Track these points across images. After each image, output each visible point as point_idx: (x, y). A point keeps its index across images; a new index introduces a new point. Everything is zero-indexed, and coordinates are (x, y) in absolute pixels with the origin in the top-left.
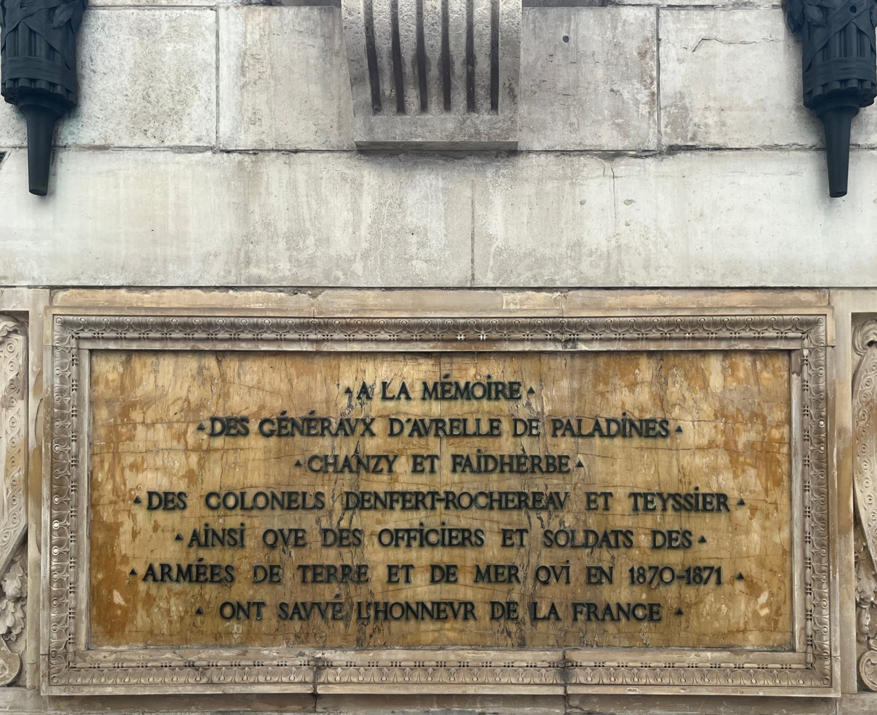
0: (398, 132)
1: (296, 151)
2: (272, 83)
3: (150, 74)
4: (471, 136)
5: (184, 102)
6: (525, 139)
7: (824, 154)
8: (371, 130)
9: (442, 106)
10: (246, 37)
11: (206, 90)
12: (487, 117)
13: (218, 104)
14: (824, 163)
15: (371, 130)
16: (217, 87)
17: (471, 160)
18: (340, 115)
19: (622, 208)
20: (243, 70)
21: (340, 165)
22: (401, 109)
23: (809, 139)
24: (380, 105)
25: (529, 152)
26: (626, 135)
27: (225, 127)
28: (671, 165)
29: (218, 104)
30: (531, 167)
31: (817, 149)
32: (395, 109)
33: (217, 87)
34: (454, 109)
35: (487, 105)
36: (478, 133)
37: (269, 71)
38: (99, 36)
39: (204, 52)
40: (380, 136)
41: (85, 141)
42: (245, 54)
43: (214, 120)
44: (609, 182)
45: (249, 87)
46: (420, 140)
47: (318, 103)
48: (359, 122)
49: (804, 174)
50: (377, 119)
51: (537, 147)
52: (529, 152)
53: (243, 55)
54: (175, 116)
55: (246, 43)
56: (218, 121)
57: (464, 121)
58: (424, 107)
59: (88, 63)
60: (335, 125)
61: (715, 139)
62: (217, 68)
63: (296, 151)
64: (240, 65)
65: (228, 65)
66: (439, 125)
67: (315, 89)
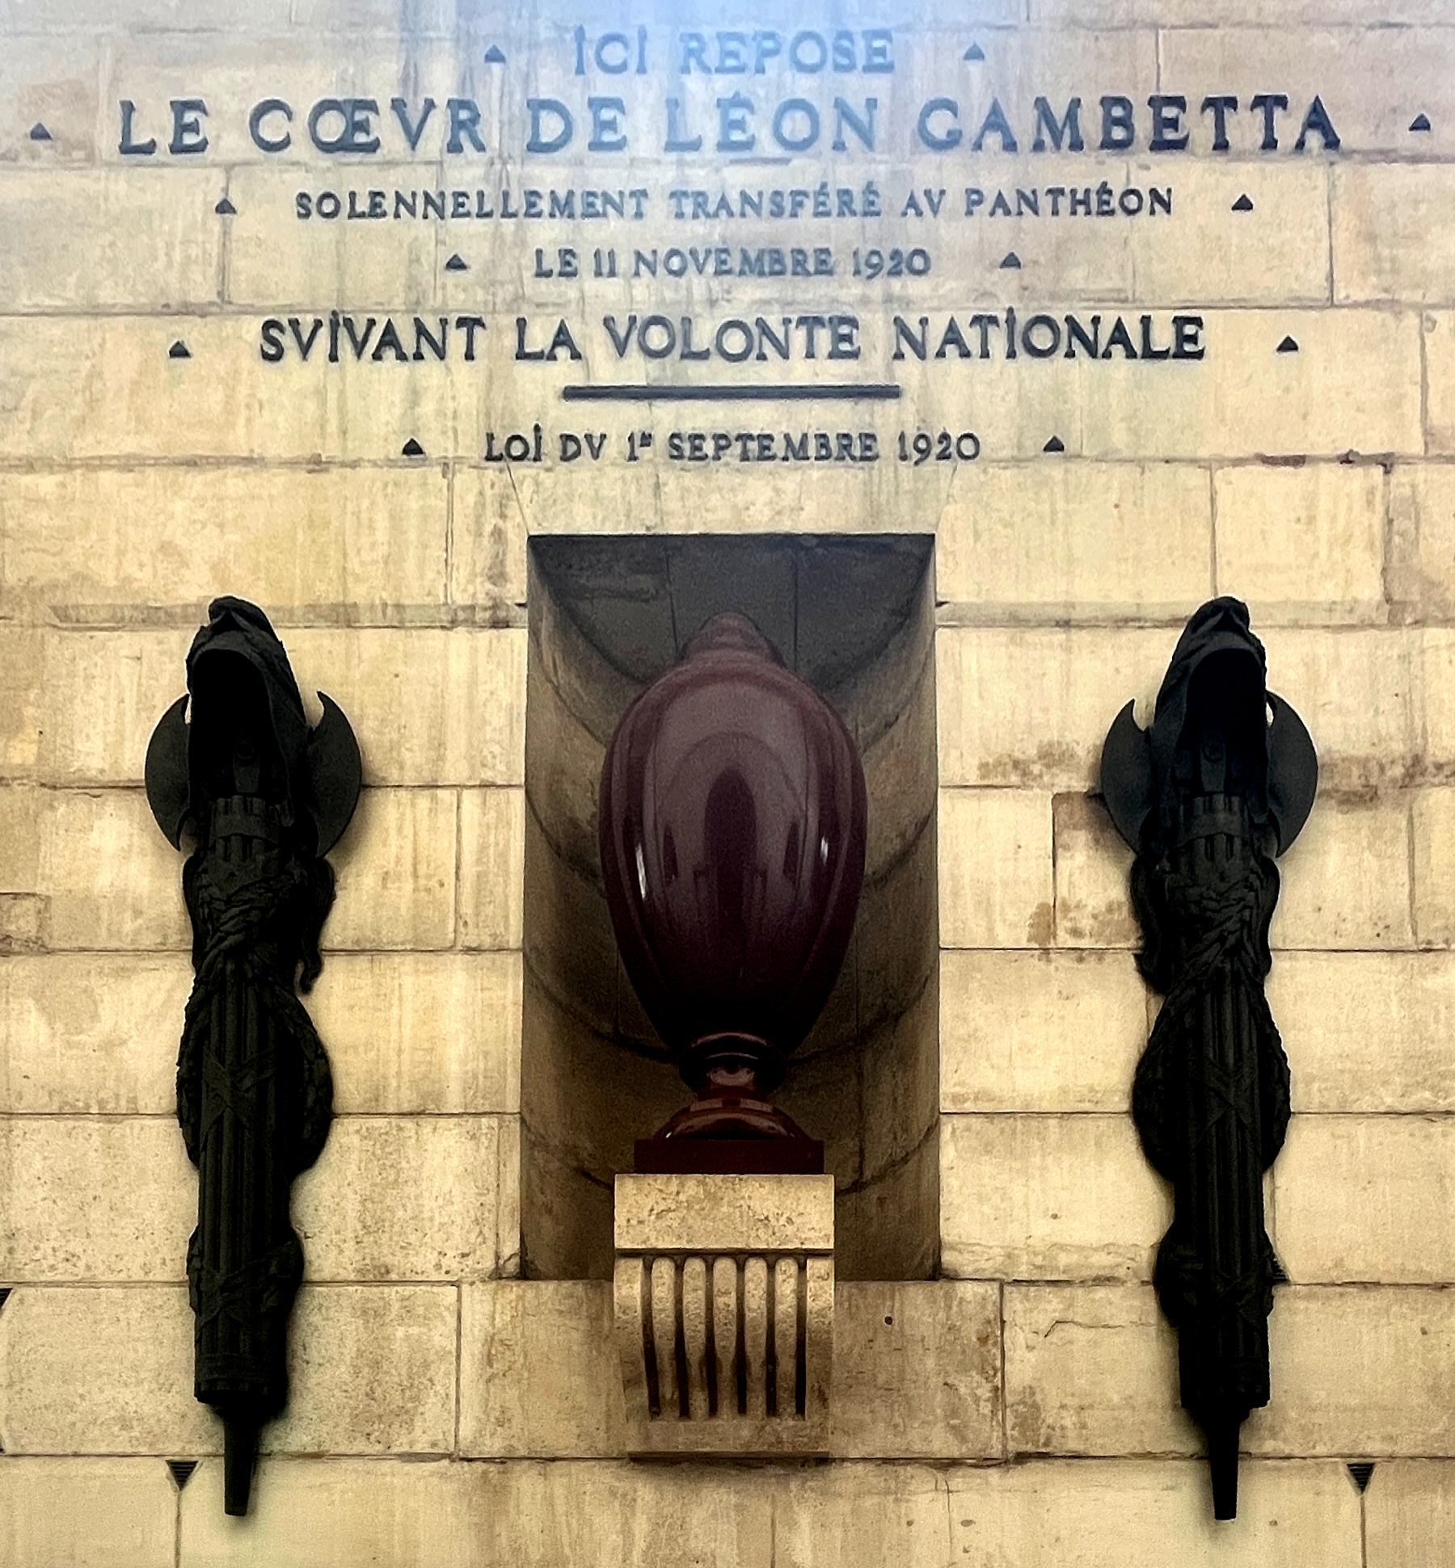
0: (680, 1439)
1: (554, 1460)
2: (526, 1375)
3: (376, 1365)
4: (771, 1445)
5: (416, 1399)
6: (836, 1444)
7: (1205, 1464)
8: (647, 1438)
9: (735, 1410)
10: (494, 1319)
11: (443, 1382)
12: (791, 1423)
13: (458, 1401)
14: (1208, 1474)
15: (647, 1438)
16: (458, 1380)
17: (771, 1470)
18: (609, 1416)
19: (960, 1530)
20: (489, 1360)
21: (605, 1477)
22: (685, 1412)
23: (1191, 1446)
24: (658, 1406)
25: (843, 1460)
26: (964, 1440)
27: (467, 1429)
28: (1020, 1477)
29: (458, 1401)
30: (846, 1478)
31: (1200, 1458)
32: (677, 1414)
33: (458, 1380)
34: (750, 1413)
35: (792, 1409)
36: (780, 1442)
37: (522, 1360)
38: (315, 1319)
39: (441, 1336)
40: (658, 1445)
41: (293, 1448)
42: (492, 1339)
43: (453, 1421)
44: (943, 1497)
45: (496, 1381)
46: (707, 1449)
47: (581, 1398)
48: (632, 1429)
49: (1176, 1494)
50: (656, 1427)
51: (854, 1454)
52: (843, 1460)
53: (490, 1340)
54: (405, 1416)
55: (494, 1327)
56: (457, 1422)
57: (763, 1427)
58: (713, 1411)
59: (300, 1352)
60: (603, 1427)
61: (1074, 1445)
62: (458, 1357)
63: (554, 1460)
64: (485, 1353)
65: (472, 1350)
66: (733, 1432)
67: (578, 1381)
